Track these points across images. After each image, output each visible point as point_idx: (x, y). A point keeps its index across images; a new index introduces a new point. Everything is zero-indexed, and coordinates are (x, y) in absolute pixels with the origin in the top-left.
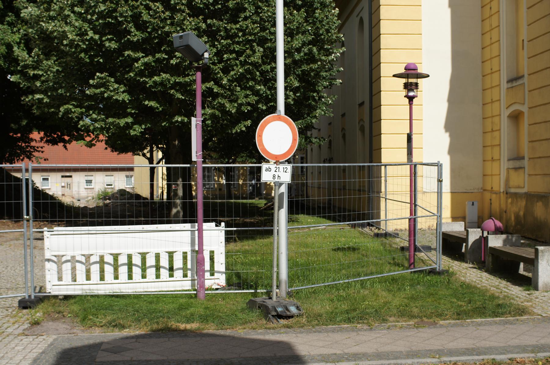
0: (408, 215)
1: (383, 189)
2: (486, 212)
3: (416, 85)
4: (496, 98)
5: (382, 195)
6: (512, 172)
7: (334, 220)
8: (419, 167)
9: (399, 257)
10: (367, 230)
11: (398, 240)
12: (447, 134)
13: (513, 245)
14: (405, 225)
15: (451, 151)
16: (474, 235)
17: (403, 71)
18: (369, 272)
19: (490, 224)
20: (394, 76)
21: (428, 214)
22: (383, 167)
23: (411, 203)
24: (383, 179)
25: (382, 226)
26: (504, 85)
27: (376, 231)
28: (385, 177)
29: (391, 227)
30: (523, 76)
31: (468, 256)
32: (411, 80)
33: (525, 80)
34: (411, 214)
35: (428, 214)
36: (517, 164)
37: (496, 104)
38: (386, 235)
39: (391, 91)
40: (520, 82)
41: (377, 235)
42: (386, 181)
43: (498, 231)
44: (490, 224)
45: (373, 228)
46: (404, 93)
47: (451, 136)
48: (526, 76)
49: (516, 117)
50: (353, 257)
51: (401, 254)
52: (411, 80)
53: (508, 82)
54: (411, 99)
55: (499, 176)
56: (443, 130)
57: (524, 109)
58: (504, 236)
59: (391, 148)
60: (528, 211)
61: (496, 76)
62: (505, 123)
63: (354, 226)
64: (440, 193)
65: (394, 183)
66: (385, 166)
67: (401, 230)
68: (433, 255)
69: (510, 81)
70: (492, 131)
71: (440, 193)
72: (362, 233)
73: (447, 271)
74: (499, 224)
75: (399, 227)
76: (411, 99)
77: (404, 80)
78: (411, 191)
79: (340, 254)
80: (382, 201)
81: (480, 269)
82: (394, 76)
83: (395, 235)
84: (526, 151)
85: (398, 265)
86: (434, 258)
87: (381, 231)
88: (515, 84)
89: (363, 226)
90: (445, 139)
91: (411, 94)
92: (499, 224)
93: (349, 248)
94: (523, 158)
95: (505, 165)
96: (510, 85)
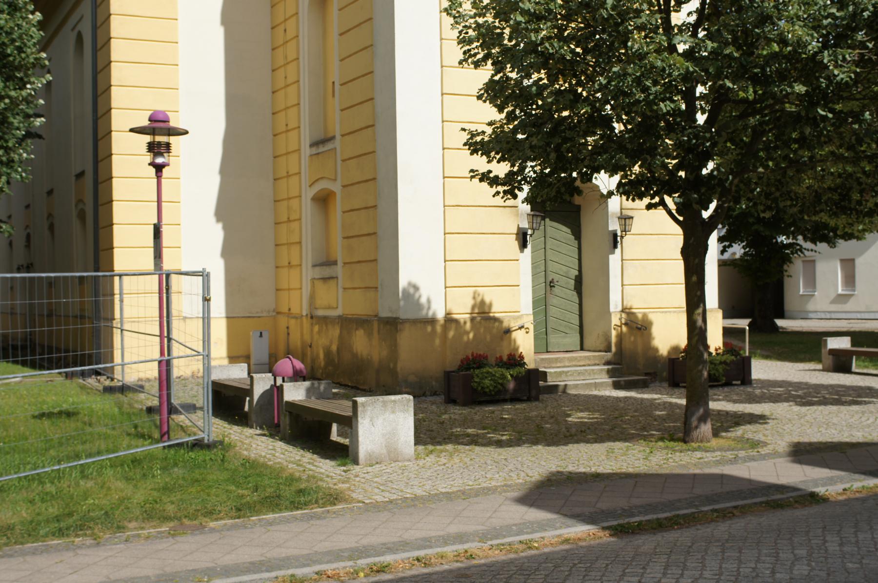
0: (157, 355)
1: (117, 315)
2: (282, 348)
3: (168, 146)
4: (293, 170)
5: (116, 323)
6: (319, 285)
7: (34, 365)
8: (173, 277)
9: (145, 423)
10: (91, 381)
11: (142, 396)
12: (220, 226)
13: (321, 397)
14: (152, 371)
15: (227, 252)
16: (262, 384)
17: (145, 123)
18: (95, 450)
19: (286, 365)
20: (132, 130)
21: (189, 352)
22: (117, 279)
23: (161, 336)
24: (117, 298)
25: (118, 375)
26: (306, 151)
27: (108, 383)
28: (121, 294)
29: (131, 376)
30: (333, 138)
31: (253, 417)
32: (159, 139)
33: (337, 143)
34: (162, 354)
35: (189, 352)
36: (327, 272)
37: (294, 180)
38: (124, 389)
39: (128, 155)
40: (329, 146)
41: (109, 390)
42: (121, 301)
43: (298, 376)
44: (286, 365)
45: (102, 378)
46: (148, 158)
47: (225, 228)
48: (338, 137)
49: (323, 200)
50: (69, 426)
51: (146, 418)
52: (159, 139)
53: (311, 146)
54: (159, 169)
55: (301, 290)
56: (213, 219)
57: (336, 187)
58: (307, 384)
59: (129, 248)
60: (344, 343)
61: (293, 135)
62: (307, 210)
63: (68, 376)
64: (206, 319)
65: (134, 305)
66: (120, 276)
67: (148, 380)
68: (198, 418)
69: (315, 144)
70: (289, 221)
71: (206, 319)
72: (83, 387)
73: (221, 443)
74: (299, 365)
75: (142, 375)
76: (159, 169)
77: (148, 138)
78: (161, 316)
79: (46, 423)
80: (117, 333)
81: (272, 436)
82: (132, 130)
83: (138, 388)
84: (339, 252)
85: (142, 436)
86: (200, 423)
87: (115, 383)
88: (321, 149)
89: (83, 374)
90: (215, 234)
91: (159, 160)
92: (299, 365)
93: (60, 413)
94: (335, 263)
95: (308, 273)
96: (314, 150)
